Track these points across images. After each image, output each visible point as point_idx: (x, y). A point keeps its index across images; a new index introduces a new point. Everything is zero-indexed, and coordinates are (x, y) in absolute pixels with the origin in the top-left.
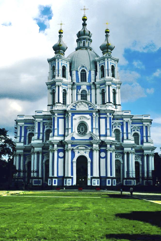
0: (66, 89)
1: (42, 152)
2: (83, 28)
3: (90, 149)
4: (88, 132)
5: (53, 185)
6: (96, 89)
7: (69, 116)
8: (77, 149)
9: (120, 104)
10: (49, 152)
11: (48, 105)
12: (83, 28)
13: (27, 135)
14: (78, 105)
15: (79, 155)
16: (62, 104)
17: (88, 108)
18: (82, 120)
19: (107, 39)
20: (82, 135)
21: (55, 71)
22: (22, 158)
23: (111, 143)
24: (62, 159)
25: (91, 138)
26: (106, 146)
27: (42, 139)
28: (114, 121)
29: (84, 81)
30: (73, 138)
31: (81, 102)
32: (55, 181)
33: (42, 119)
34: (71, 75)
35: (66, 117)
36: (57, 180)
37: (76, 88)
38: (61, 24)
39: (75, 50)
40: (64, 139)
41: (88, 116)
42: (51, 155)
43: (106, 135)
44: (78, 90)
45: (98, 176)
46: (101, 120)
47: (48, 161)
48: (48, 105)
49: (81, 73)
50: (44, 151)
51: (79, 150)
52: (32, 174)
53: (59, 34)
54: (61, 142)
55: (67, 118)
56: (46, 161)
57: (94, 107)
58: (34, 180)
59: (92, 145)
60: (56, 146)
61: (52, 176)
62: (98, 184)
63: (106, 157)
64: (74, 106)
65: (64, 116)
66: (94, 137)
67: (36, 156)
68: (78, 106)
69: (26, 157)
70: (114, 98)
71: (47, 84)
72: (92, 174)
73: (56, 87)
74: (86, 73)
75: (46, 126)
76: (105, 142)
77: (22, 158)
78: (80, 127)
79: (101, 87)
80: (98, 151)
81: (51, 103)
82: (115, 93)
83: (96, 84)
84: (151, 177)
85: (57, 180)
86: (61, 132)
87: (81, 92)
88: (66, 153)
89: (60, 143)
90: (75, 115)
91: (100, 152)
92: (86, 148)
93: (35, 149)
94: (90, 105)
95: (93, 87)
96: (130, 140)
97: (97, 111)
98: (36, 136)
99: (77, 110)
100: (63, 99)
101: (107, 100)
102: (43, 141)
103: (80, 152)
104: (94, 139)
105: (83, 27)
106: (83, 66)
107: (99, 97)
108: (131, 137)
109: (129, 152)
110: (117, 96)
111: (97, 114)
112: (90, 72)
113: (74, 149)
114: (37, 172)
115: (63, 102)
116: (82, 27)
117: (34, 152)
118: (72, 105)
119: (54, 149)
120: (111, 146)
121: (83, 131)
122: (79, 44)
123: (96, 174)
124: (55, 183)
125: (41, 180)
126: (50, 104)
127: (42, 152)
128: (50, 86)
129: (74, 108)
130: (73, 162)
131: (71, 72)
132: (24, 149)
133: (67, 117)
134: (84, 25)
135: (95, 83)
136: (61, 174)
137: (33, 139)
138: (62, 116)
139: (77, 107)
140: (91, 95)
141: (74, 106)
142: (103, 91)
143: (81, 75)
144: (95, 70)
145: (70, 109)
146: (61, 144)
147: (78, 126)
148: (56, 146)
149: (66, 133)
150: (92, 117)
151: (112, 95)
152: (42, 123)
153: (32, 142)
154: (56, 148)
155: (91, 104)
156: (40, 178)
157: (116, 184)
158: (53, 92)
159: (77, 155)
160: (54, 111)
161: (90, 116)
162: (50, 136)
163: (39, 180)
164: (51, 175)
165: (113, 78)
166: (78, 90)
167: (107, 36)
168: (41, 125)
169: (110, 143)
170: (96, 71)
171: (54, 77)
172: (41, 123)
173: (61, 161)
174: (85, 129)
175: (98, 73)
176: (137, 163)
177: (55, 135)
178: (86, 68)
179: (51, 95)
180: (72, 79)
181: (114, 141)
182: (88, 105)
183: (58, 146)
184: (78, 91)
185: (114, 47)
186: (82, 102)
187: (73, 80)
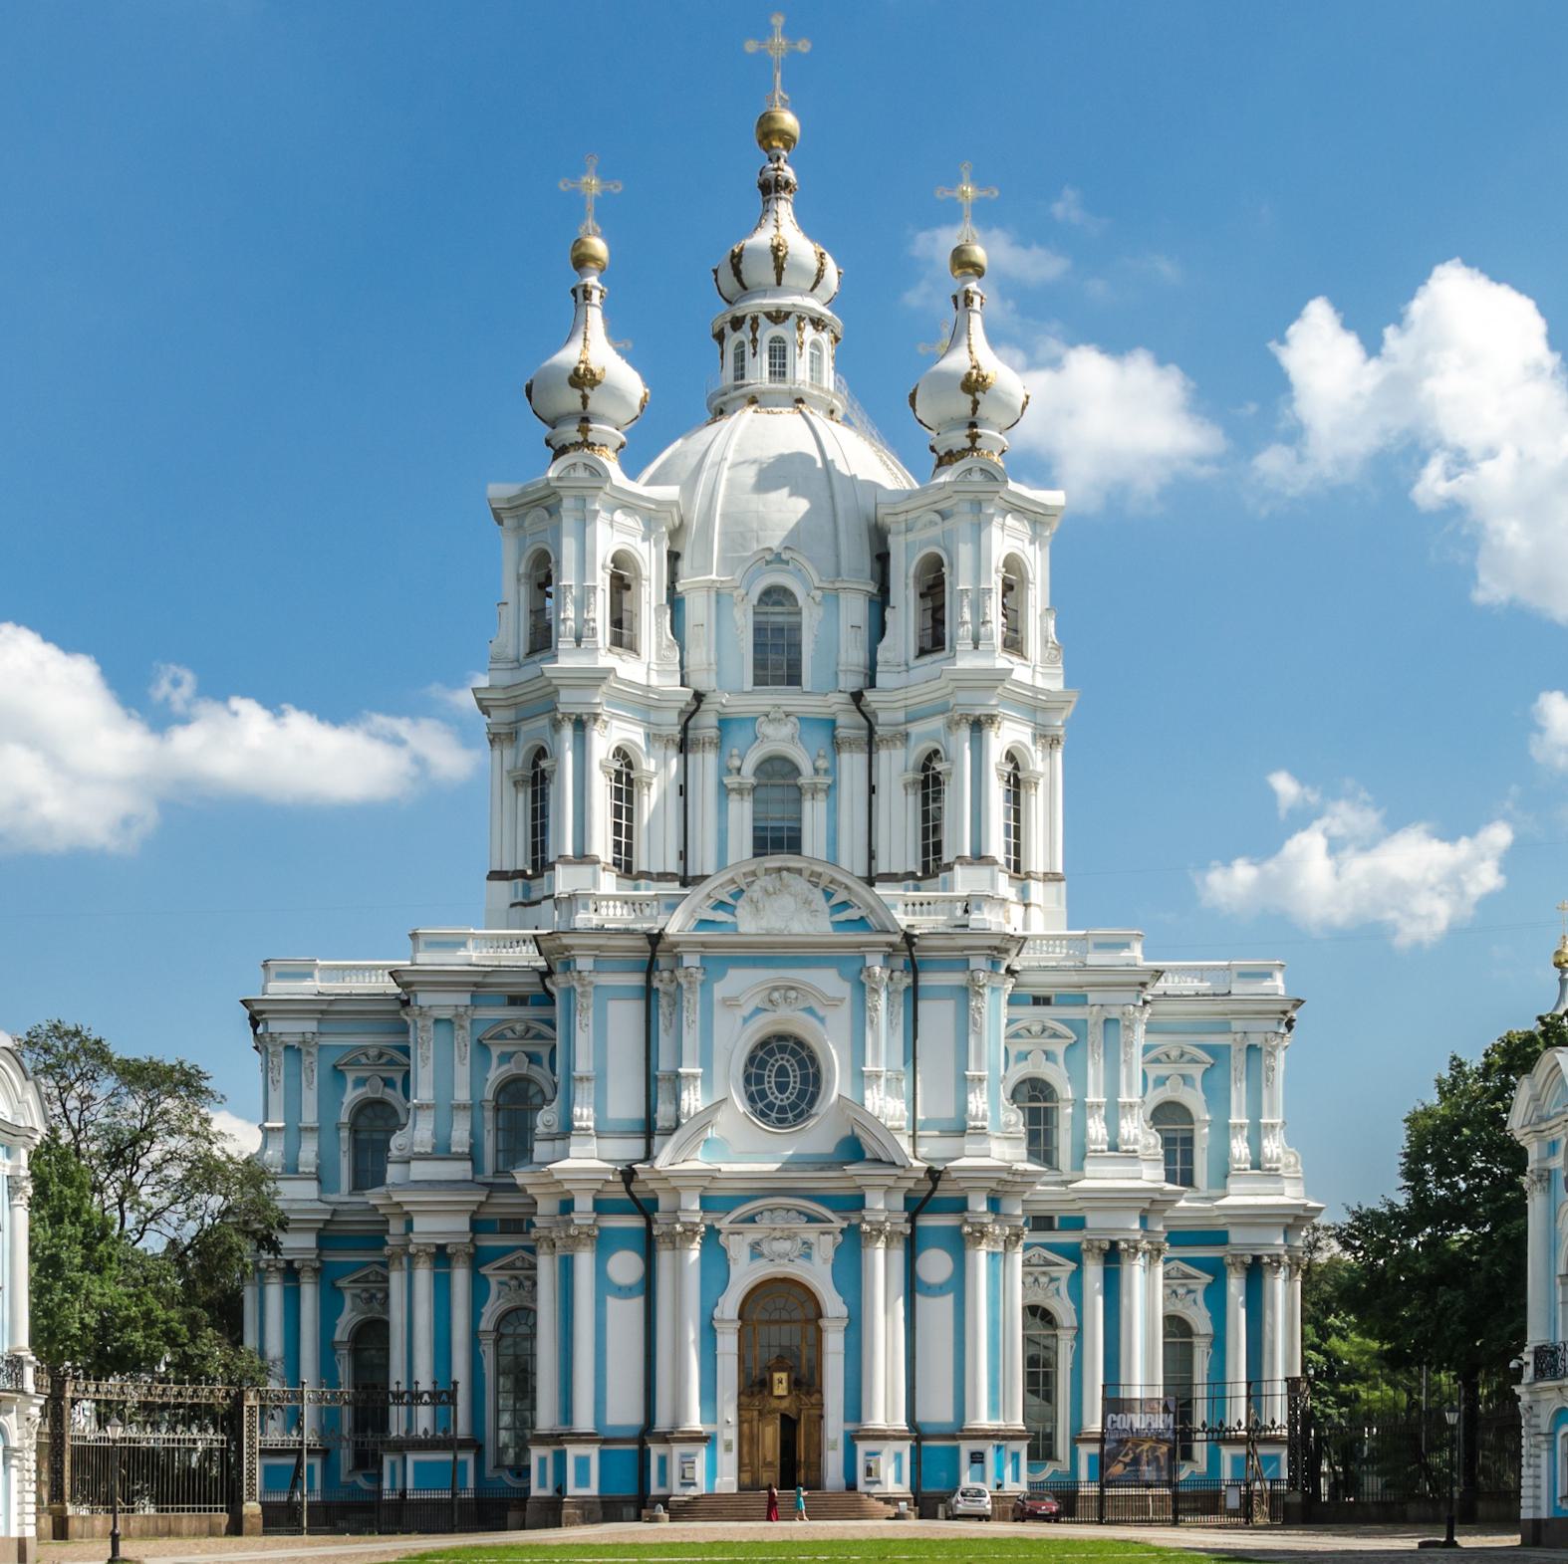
1: (472, 1251)
3: (842, 1231)
5: (572, 1490)
6: (871, 744)
7: (679, 973)
9: (1059, 869)
10: (532, 1250)
11: (496, 875)
13: (344, 1118)
14: (755, 892)
15: (764, 1270)
21: (549, 595)
22: (309, 1293)
23: (1000, 1181)
24: (637, 1304)
25: (852, 1150)
26: (960, 1206)
27: (472, 1146)
31: (780, 870)
32: (583, 1463)
33: (465, 999)
34: (677, 628)
35: (657, 989)
36: (592, 1452)
37: (713, 733)
40: (649, 1156)
41: (828, 981)
42: (546, 1268)
45: (901, 1423)
46: (923, 1006)
47: (521, 1316)
48: (496, 875)
50: (489, 1241)
52: (397, 1415)
56: (503, 1319)
58: (411, 1458)
59: (857, 1203)
60: (584, 1204)
61: (561, 1429)
62: (899, 1480)
63: (958, 1285)
65: (648, 981)
67: (423, 1276)
69: (341, 1284)
70: (1017, 819)
72: (855, 1406)
73: (556, 725)
74: (799, 613)
75: (495, 1052)
76: (954, 1175)
77: (309, 1293)
78: (763, 1064)
79: (915, 729)
80: (902, 1239)
82: (1016, 786)
83: (874, 705)
84: (1281, 1427)
85: (592, 1452)
86: (625, 1103)
88: (664, 1258)
89: (622, 1187)
91: (912, 1247)
93: (420, 1224)
95: (849, 722)
96: (1132, 1156)
97: (897, 939)
101: (958, 839)
102: (477, 1167)
103: (765, 1248)
104: (871, 1150)
107: (899, 814)
108: (1136, 1130)
110: (1037, 804)
111: (899, 962)
113: (719, 1232)
114: (443, 1397)
117: (412, 1249)
118: (709, 896)
119: (572, 1231)
120: (994, 1204)
123: (886, 1410)
124: (583, 1480)
125: (468, 1457)
126: (507, 867)
127: (472, 1251)
128: (508, 715)
130: (716, 1325)
131: (675, 601)
132: (321, 1226)
133: (672, 988)
135: (869, 696)
136: (624, 1412)
139: (743, 910)
140: (831, 790)
142: (925, 768)
144: (869, 589)
146: (628, 1190)
147: (751, 1059)
148: (584, 1204)
152: (467, 1024)
153: (393, 1172)
154: (591, 1222)
155: (847, 887)
156: (464, 1445)
157: (1031, 1485)
158: (535, 765)
159: (745, 1274)
160: (566, 940)
162: (540, 1129)
163: (461, 1456)
164: (546, 1418)
165: (1015, 659)
168: (464, 1037)
169: (993, 1185)
170: (881, 600)
171: (542, 640)
172: (462, 1027)
173: (625, 1315)
174: (805, 1079)
176: (1177, 1328)
178: (799, 572)
179: (521, 796)
181: (1015, 1173)
182: (829, 895)
183: (601, 1207)
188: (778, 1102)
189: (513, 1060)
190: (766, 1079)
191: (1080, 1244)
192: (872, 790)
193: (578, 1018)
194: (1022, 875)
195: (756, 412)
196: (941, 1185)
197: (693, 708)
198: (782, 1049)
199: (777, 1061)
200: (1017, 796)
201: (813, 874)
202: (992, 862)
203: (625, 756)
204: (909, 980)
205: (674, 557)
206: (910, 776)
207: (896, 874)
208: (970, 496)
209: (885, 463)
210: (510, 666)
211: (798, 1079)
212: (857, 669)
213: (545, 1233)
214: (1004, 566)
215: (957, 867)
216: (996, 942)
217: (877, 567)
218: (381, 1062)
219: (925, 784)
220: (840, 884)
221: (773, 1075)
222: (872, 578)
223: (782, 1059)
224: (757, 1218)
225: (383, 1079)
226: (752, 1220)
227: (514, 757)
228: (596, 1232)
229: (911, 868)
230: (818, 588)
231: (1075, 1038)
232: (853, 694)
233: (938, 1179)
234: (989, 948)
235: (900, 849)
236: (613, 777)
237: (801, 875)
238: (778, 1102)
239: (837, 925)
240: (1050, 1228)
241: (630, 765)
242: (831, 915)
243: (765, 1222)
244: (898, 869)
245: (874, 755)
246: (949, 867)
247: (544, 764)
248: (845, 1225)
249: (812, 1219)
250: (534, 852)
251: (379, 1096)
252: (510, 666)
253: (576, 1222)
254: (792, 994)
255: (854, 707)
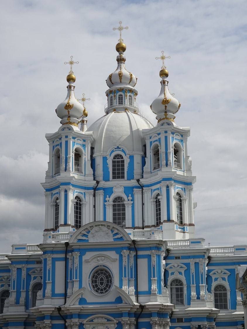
0: (82, 196)
2: (118, 68)
3: (117, 324)
4: (113, 288)
8: (90, 324)
12: (119, 67)
14: (92, 231)
16: (73, 227)
17: (113, 239)
18: (101, 263)
19: (163, 91)
20: (102, 293)
23: (160, 308)
25: (119, 300)
28: (169, 261)
29: (119, 178)
30: (82, 301)
31: (99, 225)
35: (68, 258)
38: (71, 63)
39: (105, 114)
41: (113, 255)
43: (149, 293)
44: (108, 196)
46: (139, 261)
49: (114, 162)
51: (94, 326)
53: (67, 84)
54: (59, 309)
55: (71, 259)
57: (124, 235)
64: (84, 235)
65: (66, 256)
66: (125, 298)
68: (92, 234)
71: (43, 186)
75: (32, 276)
76: (147, 307)
78: (96, 277)
80: (134, 326)
81: (51, 226)
86: (59, 289)
87: (114, 201)
89: (57, 312)
90: (87, 253)
92: (108, 320)
94: (116, 231)
98: (12, 298)
99: (89, 242)
100: (76, 217)
101: (164, 217)
105: (118, 66)
106: (118, 148)
109: (202, 326)
112: (131, 158)
113: (83, 324)
115: (76, 222)
116: (117, 65)
118: (81, 233)
119: (44, 325)
121: (104, 286)
122: (111, 100)
126: (49, 228)
129: (84, 238)
134: (120, 60)
135: (141, 180)
137: (8, 303)
138: (63, 256)
139: (90, 235)
141: (84, 235)
142: (156, 198)
143: (114, 166)
144: (142, 154)
145: (76, 241)
146: (59, 313)
149: (69, 291)
150: (121, 256)
151: (174, 204)
152: (25, 269)
154: (49, 322)
155: (117, 229)
160: (44, 246)
161: (117, 253)
166: (108, 196)
167: (163, 83)
172: (24, 270)
174: (108, 281)
175: (147, 160)
177: (46, 295)
178: (123, 151)
180: (94, 175)
182: (112, 231)
184: (107, 199)
185: (180, 105)
186: (100, 226)
187: (97, 176)
188: (101, 288)
189: (37, 278)
190: (97, 282)
191: (190, 326)
192: (143, 204)
193: (47, 267)
194: (183, 225)
195: (115, 113)
196: (144, 310)
197: (96, 185)
198: (102, 273)
199: (100, 276)
200: (181, 205)
201: (108, 226)
202: (173, 221)
203: (79, 198)
204: (135, 253)
205: (92, 148)
206: (152, 200)
207: (150, 226)
208: (164, 129)
209: (147, 123)
210: (50, 177)
211: (106, 281)
212: (139, 174)
213: (38, 326)
214: (174, 146)
215: (163, 223)
216: (158, 242)
217: (144, 148)
218: (8, 280)
219: (156, 202)
220: (115, 228)
221: (99, 280)
222: (142, 151)
223: (102, 276)
224: (93, 320)
225: (8, 285)
226: (92, 321)
227: (51, 200)
228: (51, 325)
229: (153, 224)
230: (128, 154)
231: (187, 268)
232: (137, 180)
233: (143, 308)
234: (156, 244)
235: (150, 220)
236: (75, 203)
237: (105, 226)
238: (101, 288)
239: (114, 239)
240: (182, 321)
241: (80, 201)
242: (113, 237)
243: (95, 321)
244: (150, 224)
245: (143, 195)
246: (162, 223)
247: (57, 201)
248: (118, 322)
249: (108, 320)
250: (56, 224)
251: (7, 289)
252: (50, 177)
253: (46, 322)
254: (103, 258)
255: (137, 183)
